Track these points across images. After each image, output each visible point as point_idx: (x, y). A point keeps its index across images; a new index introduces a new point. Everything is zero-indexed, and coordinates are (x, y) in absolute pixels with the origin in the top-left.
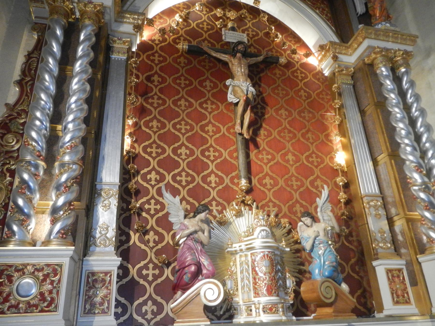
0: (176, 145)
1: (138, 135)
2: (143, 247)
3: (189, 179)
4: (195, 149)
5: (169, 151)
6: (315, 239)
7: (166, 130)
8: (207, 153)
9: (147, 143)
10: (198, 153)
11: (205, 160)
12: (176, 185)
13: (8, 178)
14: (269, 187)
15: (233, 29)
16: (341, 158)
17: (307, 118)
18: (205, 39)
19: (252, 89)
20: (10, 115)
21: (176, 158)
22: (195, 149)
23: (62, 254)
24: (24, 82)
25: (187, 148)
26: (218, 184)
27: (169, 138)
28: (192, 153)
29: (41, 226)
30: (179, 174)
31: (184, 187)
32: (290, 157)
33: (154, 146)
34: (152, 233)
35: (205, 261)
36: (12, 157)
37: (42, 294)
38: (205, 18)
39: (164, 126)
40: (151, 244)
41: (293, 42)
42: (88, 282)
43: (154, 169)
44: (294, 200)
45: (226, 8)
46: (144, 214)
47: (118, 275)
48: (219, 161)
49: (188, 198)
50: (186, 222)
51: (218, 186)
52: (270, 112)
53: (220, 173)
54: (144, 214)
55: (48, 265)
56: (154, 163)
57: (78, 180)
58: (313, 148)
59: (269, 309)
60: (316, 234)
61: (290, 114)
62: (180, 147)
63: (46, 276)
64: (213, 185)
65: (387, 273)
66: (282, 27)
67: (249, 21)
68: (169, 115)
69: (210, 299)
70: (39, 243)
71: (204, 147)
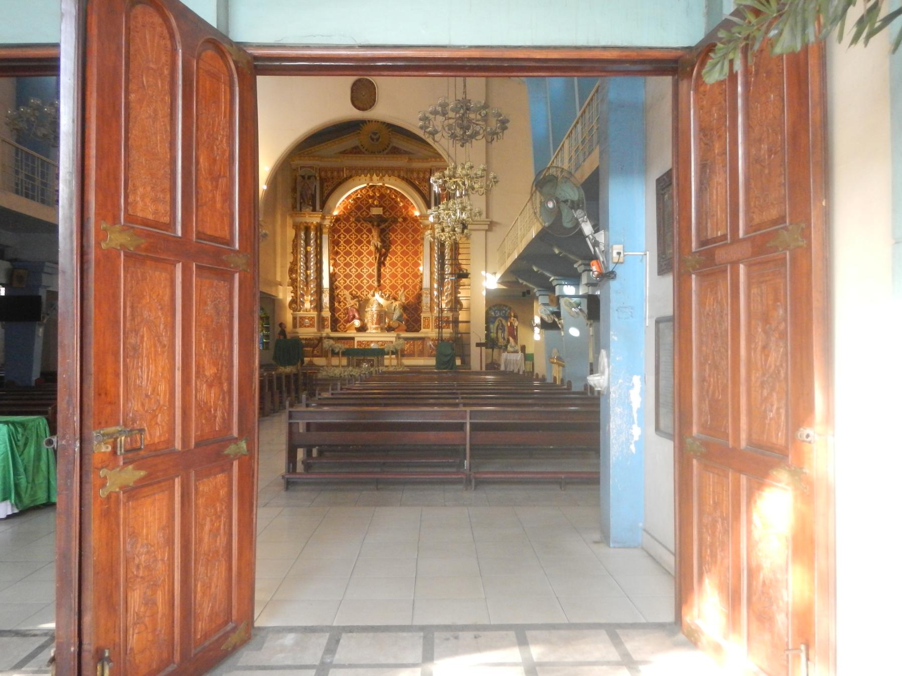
1: (335, 265)
5: (348, 270)
15: (376, 206)
16: (421, 268)
19: (379, 244)
23: (314, 314)
27: (347, 265)
29: (307, 305)
32: (399, 270)
35: (357, 315)
52: (393, 247)
57: (316, 292)
58: (410, 265)
59: (376, 329)
66: (403, 197)
68: (348, 253)
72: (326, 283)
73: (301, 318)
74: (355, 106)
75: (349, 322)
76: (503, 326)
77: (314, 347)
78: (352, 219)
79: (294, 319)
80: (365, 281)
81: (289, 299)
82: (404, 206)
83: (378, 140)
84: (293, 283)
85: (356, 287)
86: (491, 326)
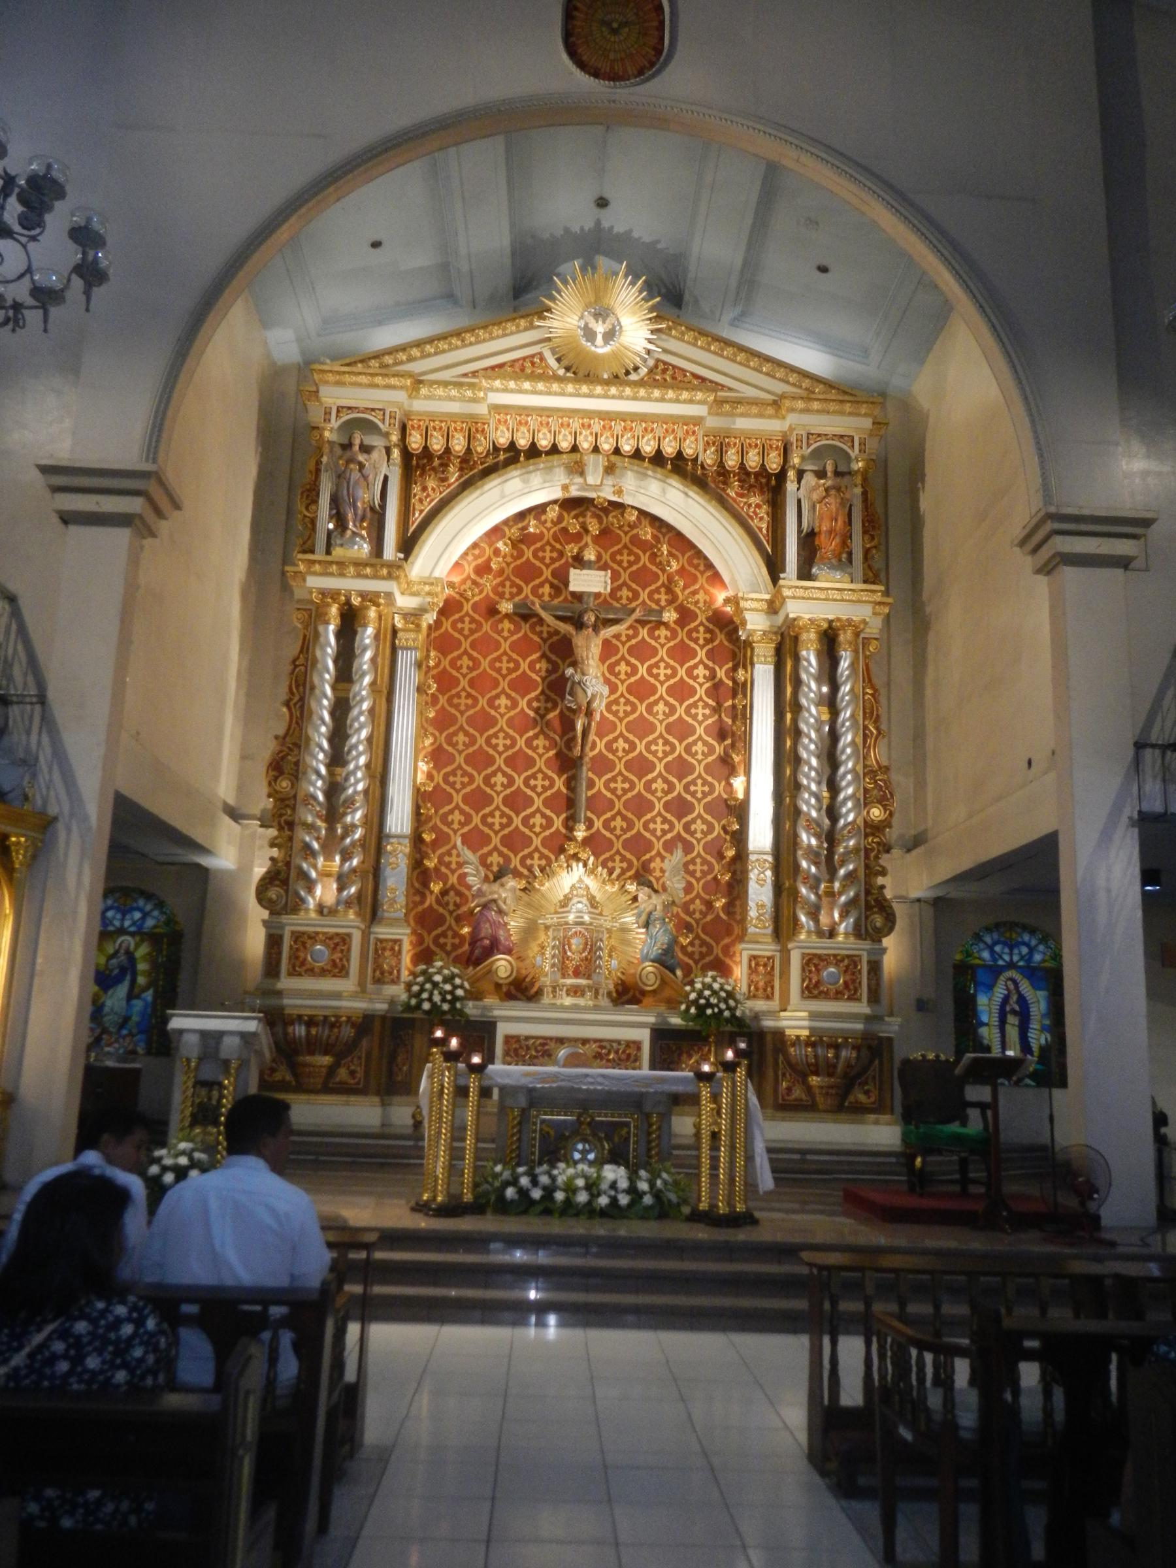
0: (490, 770)
1: (438, 756)
2: (441, 910)
3: (504, 820)
4: (516, 776)
6: (650, 914)
7: (475, 747)
8: (532, 782)
9: (449, 769)
10: (519, 781)
11: (529, 792)
12: (486, 830)
13: (288, 833)
14: (618, 832)
17: (700, 718)
18: (547, 580)
20: (281, 751)
21: (488, 790)
22: (516, 776)
24: (292, 704)
25: (504, 774)
26: (544, 828)
28: (511, 781)
30: (492, 814)
31: (496, 833)
32: (659, 785)
33: (459, 773)
34: (452, 893)
36: (287, 806)
37: (333, 961)
38: (548, 536)
39: (473, 741)
40: (451, 907)
41: (702, 568)
42: (376, 950)
43: (457, 807)
44: (653, 853)
45: (587, 509)
46: (443, 869)
47: (411, 943)
48: (549, 793)
49: (502, 848)
50: (485, 887)
51: (544, 831)
53: (548, 812)
54: (443, 869)
55: (337, 934)
56: (458, 798)
60: (650, 908)
61: (673, 710)
62: (494, 774)
63: (337, 945)
64: (537, 829)
65: (750, 961)
66: (680, 541)
67: (626, 533)
69: (504, 976)
70: (325, 911)
71: (529, 773)
72: (399, 819)
73: (297, 937)
74: (582, 65)
75: (477, 962)
76: (1022, 1000)
77: (342, 1052)
78: (506, 607)
79: (273, 942)
80: (538, 820)
81: (259, 870)
82: (682, 571)
83: (610, 336)
84: (284, 817)
85: (508, 841)
86: (982, 1000)
